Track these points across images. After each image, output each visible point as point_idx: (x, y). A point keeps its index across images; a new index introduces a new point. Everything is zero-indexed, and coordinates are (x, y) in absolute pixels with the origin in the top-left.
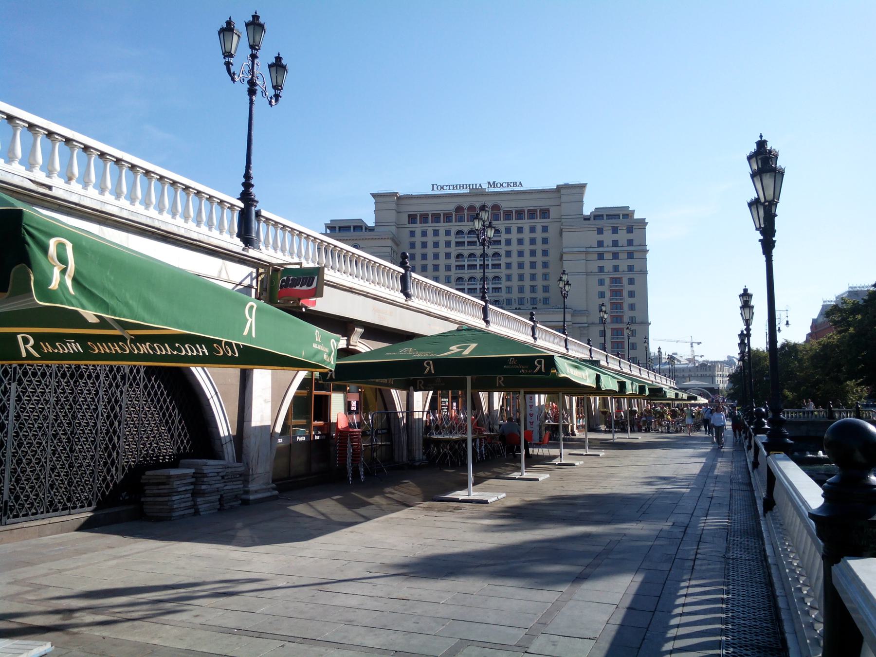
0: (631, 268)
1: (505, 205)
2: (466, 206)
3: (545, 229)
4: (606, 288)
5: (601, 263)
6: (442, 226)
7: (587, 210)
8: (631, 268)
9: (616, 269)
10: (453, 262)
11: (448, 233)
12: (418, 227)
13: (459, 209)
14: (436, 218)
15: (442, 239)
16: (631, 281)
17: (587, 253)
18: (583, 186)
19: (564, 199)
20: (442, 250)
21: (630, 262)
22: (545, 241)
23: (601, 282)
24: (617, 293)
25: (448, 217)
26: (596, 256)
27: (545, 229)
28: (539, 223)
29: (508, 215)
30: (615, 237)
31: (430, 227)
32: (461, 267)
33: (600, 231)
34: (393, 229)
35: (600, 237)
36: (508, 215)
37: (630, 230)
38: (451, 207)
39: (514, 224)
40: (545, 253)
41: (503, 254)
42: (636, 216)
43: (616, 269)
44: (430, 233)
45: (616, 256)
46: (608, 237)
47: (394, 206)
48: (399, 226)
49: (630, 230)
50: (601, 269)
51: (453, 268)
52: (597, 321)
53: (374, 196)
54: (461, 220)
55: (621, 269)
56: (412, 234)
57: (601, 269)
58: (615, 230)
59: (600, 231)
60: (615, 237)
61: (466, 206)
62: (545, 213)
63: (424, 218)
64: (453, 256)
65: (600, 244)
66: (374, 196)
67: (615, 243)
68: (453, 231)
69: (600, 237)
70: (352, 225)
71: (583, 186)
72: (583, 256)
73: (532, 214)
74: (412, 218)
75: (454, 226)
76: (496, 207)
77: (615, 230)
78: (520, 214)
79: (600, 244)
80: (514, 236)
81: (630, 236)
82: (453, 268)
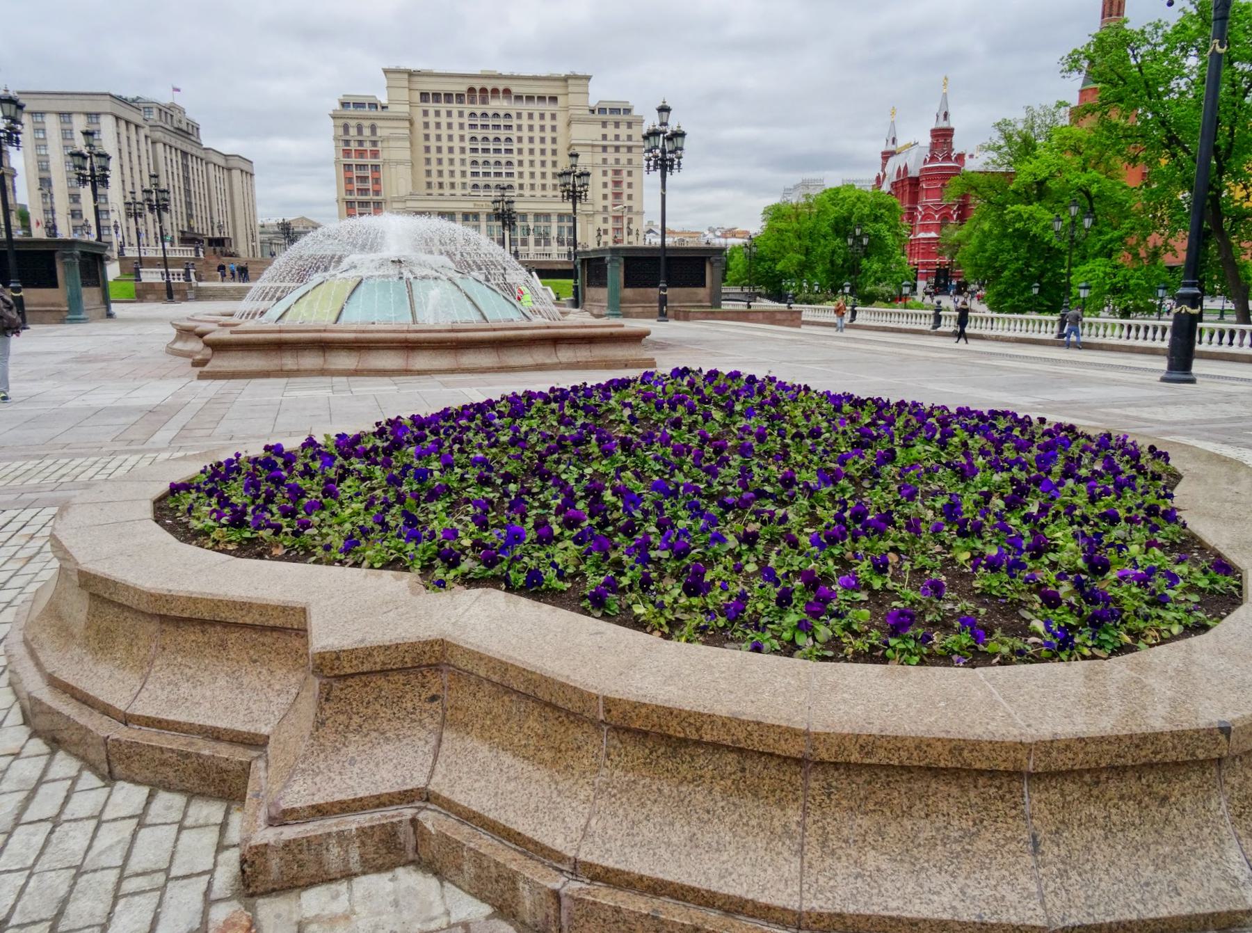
0: (630, 161)
1: (515, 90)
2: (478, 88)
3: (553, 117)
4: (609, 178)
5: (604, 155)
6: (455, 107)
7: (593, 103)
8: (630, 161)
9: (617, 161)
10: (468, 145)
11: (461, 114)
12: (431, 106)
13: (471, 90)
14: (448, 97)
15: (455, 120)
16: (630, 173)
17: (593, 146)
18: (588, 78)
19: (570, 89)
20: (456, 132)
21: (629, 156)
22: (554, 128)
23: (605, 173)
24: (617, 184)
25: (460, 97)
26: (600, 149)
27: (553, 117)
28: (547, 108)
29: (519, 98)
30: (617, 131)
31: (443, 107)
32: (474, 150)
33: (604, 124)
34: (406, 108)
35: (604, 131)
36: (519, 98)
37: (630, 125)
38: (463, 88)
39: (524, 107)
40: (554, 140)
41: (515, 139)
42: (635, 112)
43: (617, 161)
44: (443, 113)
45: (617, 149)
46: (611, 131)
47: (406, 84)
48: (411, 104)
49: (630, 125)
50: (605, 161)
51: (468, 151)
52: (601, 209)
53: (386, 71)
54: (472, 102)
55: (622, 162)
56: (426, 113)
57: (605, 161)
58: (617, 125)
59: (604, 124)
60: (617, 131)
61: (478, 88)
62: (554, 99)
63: (437, 97)
64: (467, 138)
65: (604, 137)
66: (386, 71)
67: (617, 137)
68: (466, 113)
69: (604, 131)
70: (366, 101)
71: (588, 78)
72: (589, 149)
73: (541, 98)
74: (424, 96)
75: (467, 108)
76: (507, 92)
77: (617, 125)
78: (530, 98)
79: (604, 137)
80: (525, 122)
81: (630, 132)
82: (468, 151)
